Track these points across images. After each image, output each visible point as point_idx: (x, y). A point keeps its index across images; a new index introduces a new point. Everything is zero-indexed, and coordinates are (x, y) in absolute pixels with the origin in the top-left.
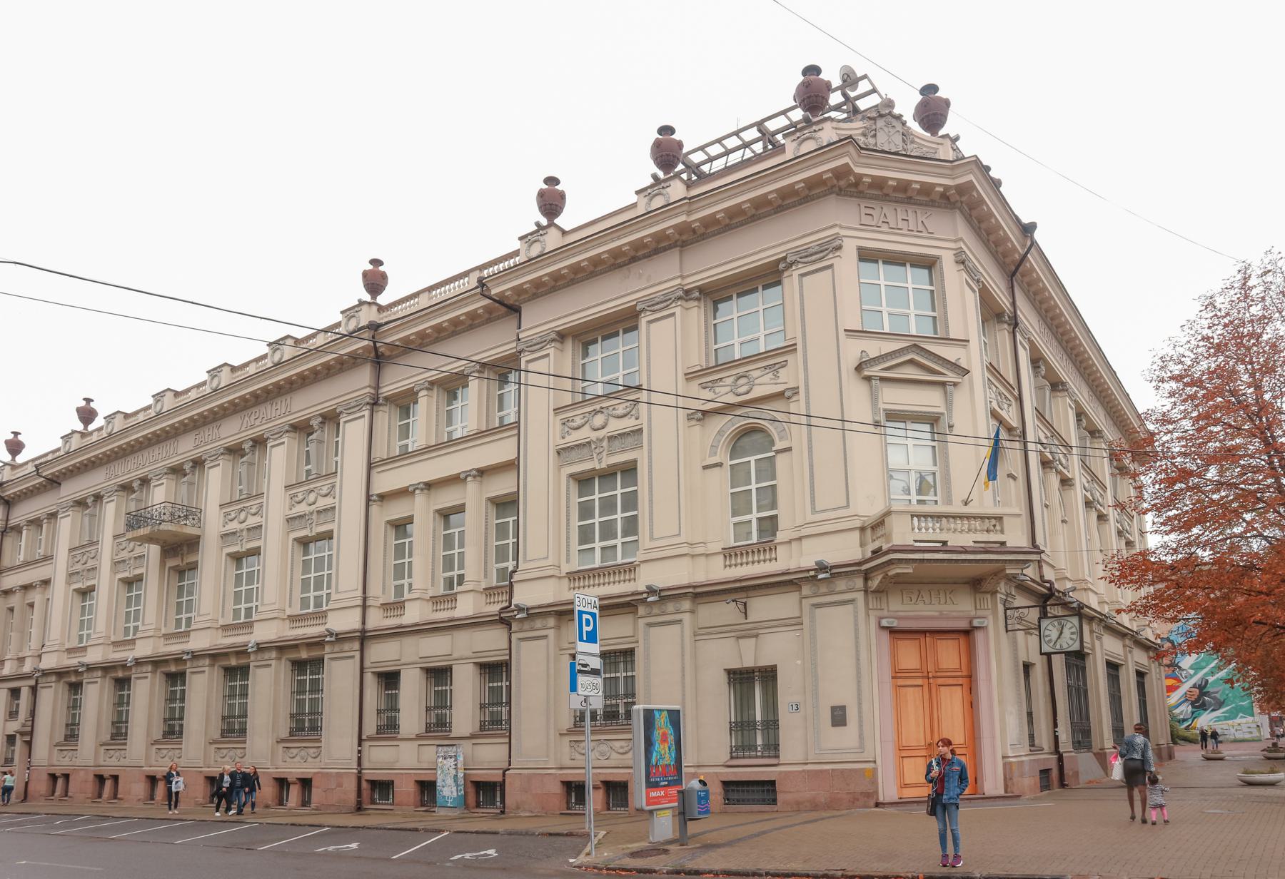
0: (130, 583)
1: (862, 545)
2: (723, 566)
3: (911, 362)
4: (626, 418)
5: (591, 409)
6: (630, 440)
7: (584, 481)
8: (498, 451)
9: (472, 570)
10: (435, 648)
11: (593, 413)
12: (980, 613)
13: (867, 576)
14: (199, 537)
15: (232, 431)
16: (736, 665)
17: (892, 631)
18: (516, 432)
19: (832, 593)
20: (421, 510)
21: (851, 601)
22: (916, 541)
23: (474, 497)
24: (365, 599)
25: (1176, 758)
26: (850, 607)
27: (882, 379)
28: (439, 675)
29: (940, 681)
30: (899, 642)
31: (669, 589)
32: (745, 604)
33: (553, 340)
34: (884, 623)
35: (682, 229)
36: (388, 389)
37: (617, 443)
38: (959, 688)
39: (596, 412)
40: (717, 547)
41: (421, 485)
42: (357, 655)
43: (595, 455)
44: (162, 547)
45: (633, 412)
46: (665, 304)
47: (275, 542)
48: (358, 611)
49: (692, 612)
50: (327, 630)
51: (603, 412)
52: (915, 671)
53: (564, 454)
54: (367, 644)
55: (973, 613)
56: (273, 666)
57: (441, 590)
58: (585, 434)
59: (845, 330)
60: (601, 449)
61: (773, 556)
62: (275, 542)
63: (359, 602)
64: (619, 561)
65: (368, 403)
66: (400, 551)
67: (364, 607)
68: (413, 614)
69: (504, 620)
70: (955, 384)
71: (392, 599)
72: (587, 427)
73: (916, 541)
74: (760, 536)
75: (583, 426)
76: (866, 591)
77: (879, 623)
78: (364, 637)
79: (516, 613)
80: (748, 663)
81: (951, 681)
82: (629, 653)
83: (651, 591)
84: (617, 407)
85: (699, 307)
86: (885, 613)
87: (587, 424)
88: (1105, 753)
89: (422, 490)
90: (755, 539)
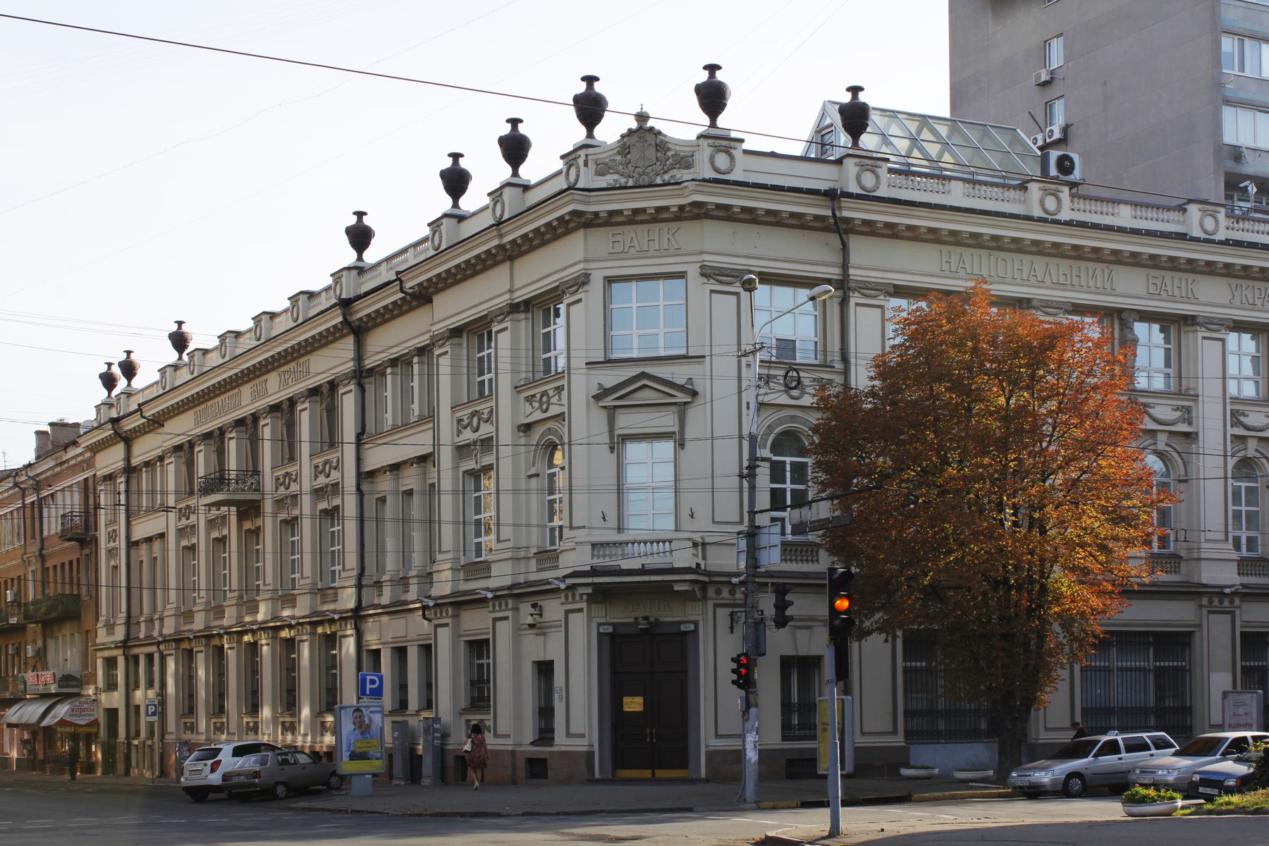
5: (470, 411)
14: (259, 501)
18: (431, 425)
28: (401, 652)
34: (601, 630)
35: (501, 247)
36: (369, 362)
78: (357, 616)
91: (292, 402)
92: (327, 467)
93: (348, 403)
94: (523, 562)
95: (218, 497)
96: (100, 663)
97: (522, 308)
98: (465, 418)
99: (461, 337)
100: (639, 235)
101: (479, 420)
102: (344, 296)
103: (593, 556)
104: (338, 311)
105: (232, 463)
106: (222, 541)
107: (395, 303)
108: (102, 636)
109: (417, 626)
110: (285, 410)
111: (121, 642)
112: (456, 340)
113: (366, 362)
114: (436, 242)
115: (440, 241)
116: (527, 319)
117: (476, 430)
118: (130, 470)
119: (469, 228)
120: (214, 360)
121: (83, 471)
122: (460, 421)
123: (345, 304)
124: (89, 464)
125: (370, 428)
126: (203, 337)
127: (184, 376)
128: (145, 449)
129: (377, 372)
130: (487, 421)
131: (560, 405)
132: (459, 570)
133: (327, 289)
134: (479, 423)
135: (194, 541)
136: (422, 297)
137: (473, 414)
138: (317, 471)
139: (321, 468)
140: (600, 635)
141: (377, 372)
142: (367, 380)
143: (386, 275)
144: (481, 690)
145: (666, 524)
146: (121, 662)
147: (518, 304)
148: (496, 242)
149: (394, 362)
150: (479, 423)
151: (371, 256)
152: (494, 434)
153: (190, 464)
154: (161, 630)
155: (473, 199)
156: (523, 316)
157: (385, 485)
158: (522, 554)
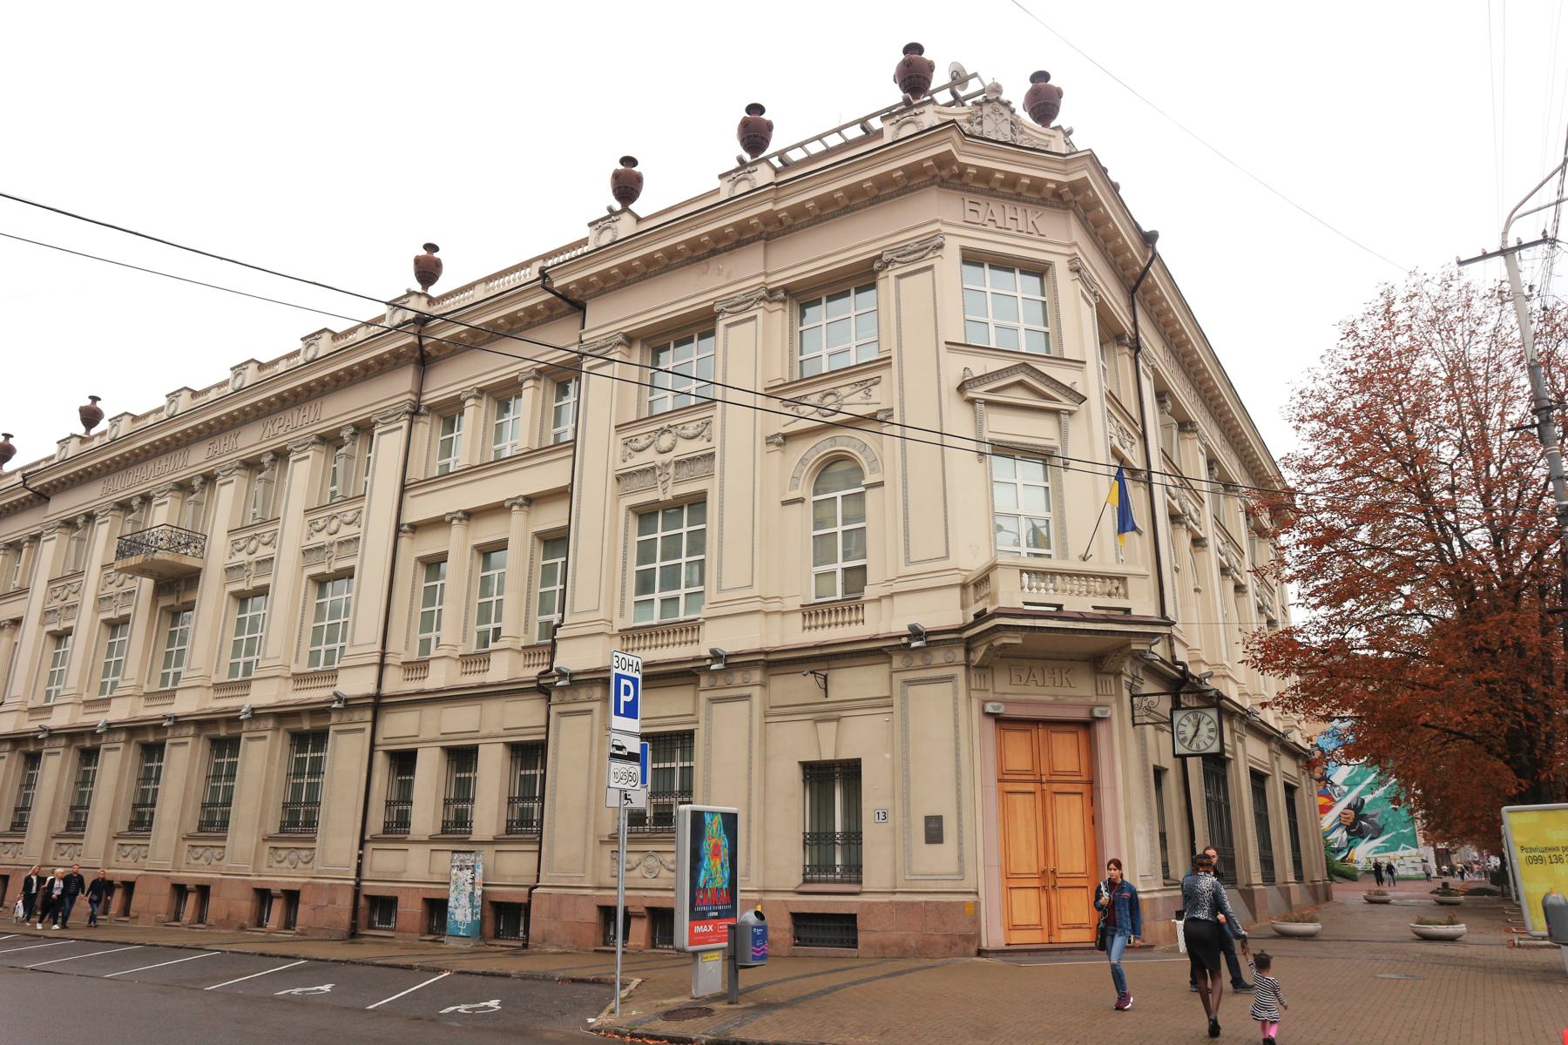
1: (964, 606)
2: (801, 628)
3: (1020, 384)
4: (697, 439)
5: (657, 427)
6: (699, 466)
7: (645, 515)
9: (510, 624)
10: (459, 721)
11: (659, 433)
12: (1102, 700)
13: (969, 646)
16: (812, 757)
17: (999, 720)
19: (928, 667)
20: (458, 544)
21: (950, 679)
22: (1026, 604)
23: (519, 530)
24: (383, 655)
25: (1335, 900)
26: (948, 686)
27: (988, 403)
29: (1056, 787)
30: (1006, 733)
31: (737, 655)
32: (826, 677)
33: (620, 344)
34: (989, 708)
37: (685, 470)
38: (1078, 798)
39: (663, 431)
40: (794, 604)
41: (460, 515)
42: (368, 727)
43: (659, 483)
45: (705, 433)
46: (746, 305)
48: (374, 671)
49: (763, 685)
50: (335, 694)
51: (671, 432)
52: (1026, 772)
53: (624, 481)
54: (382, 713)
55: (1093, 699)
56: (269, 738)
57: (472, 647)
58: (649, 457)
59: (947, 343)
60: (667, 477)
61: (860, 617)
63: (377, 659)
64: (682, 617)
65: (407, 412)
66: (430, 596)
67: (382, 666)
68: (439, 677)
69: (542, 688)
70: (1070, 413)
71: (416, 657)
72: (652, 449)
73: (1026, 604)
74: (846, 592)
75: (648, 447)
76: (967, 666)
77: (983, 708)
78: (378, 705)
79: (556, 679)
80: (828, 755)
81: (1068, 788)
82: (686, 738)
83: (716, 656)
84: (686, 425)
85: (784, 311)
86: (990, 695)
87: (652, 447)
88: (1252, 891)
90: (839, 597)
100: (1001, 212)
109: (524, 716)
132: (611, 636)
147: (772, 292)
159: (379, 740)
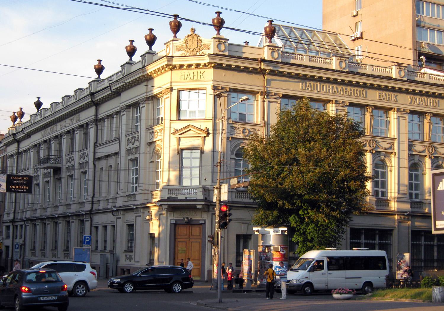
0: (48, 182)
5: (131, 137)
8: (112, 148)
15: (68, 124)
18: (118, 141)
28: (105, 227)
34: (171, 222)
36: (100, 116)
44: (54, 170)
47: (77, 174)
62: (77, 174)
63: (91, 200)
67: (92, 202)
68: (101, 207)
78: (91, 213)
89: (105, 158)
91: (73, 130)
92: (84, 155)
93: (92, 132)
94: (146, 194)
95: (46, 165)
96: (4, 228)
97: (150, 99)
98: (130, 139)
99: (130, 109)
101: (135, 140)
102: (92, 92)
103: (168, 194)
104: (89, 97)
105: (53, 153)
106: (48, 182)
107: (108, 95)
108: (6, 218)
110: (70, 133)
111: (12, 220)
112: (129, 110)
113: (99, 116)
114: (123, 73)
115: (124, 72)
116: (152, 103)
117: (133, 144)
118: (19, 154)
119: (134, 68)
120: (49, 113)
121: (3, 153)
122: (128, 140)
123: (92, 94)
124: (5, 150)
125: (99, 142)
126: (46, 105)
127: (38, 118)
128: (25, 145)
129: (102, 120)
130: (137, 141)
131: (161, 136)
133: (87, 88)
134: (134, 141)
135: (38, 182)
136: (117, 93)
137: (133, 138)
138: (81, 157)
139: (82, 156)
140: (171, 224)
141: (102, 120)
142: (99, 123)
143: (106, 84)
144: (131, 243)
145: (196, 182)
146: (11, 227)
147: (149, 97)
148: (141, 74)
149: (108, 117)
150: (134, 141)
151: (103, 76)
152: (139, 146)
153: (39, 152)
154: (25, 216)
155: (136, 58)
156: (150, 102)
157: (103, 164)
158: (146, 192)
159: (93, 224)
